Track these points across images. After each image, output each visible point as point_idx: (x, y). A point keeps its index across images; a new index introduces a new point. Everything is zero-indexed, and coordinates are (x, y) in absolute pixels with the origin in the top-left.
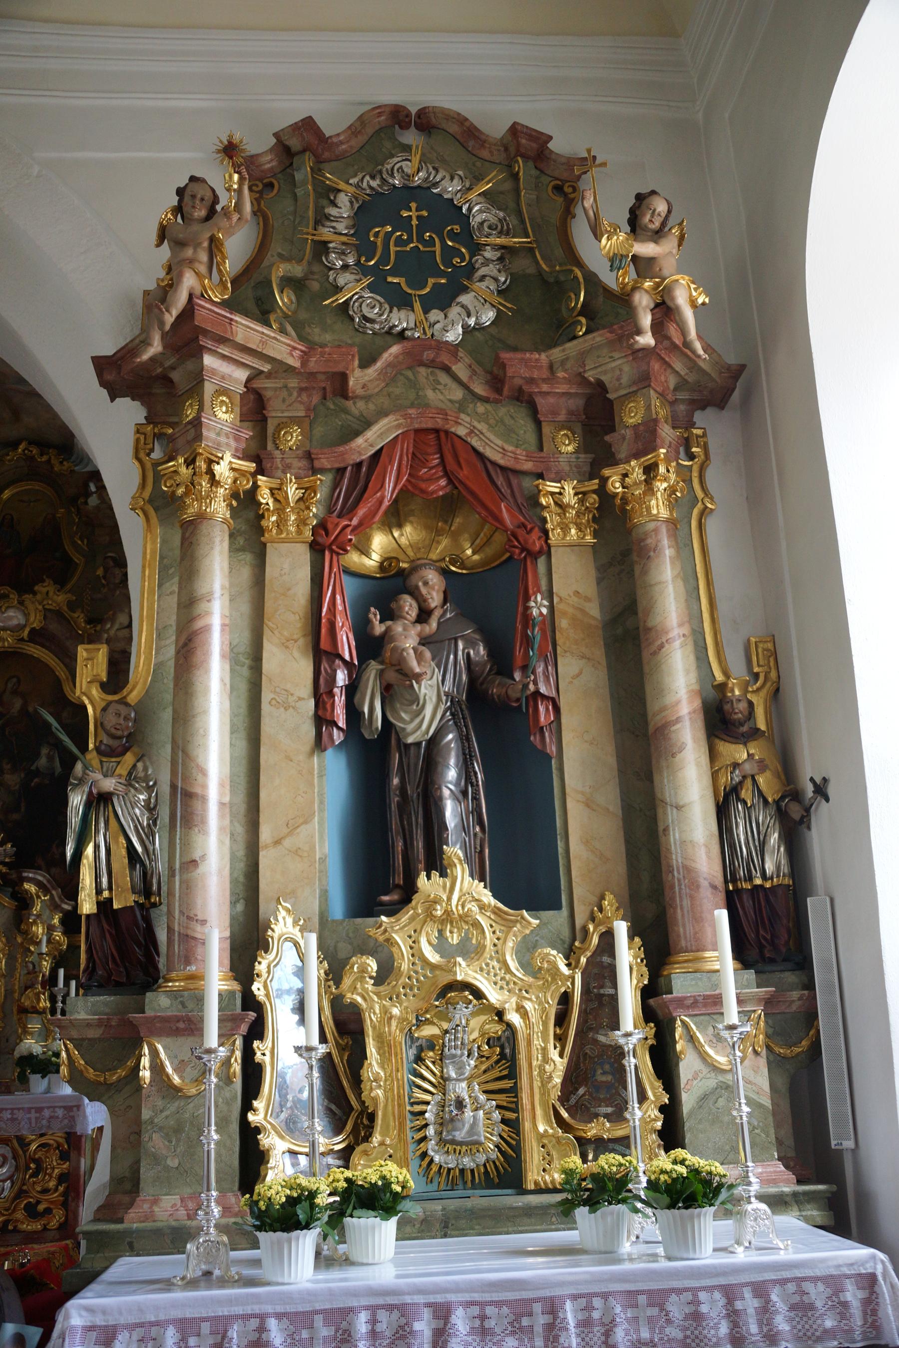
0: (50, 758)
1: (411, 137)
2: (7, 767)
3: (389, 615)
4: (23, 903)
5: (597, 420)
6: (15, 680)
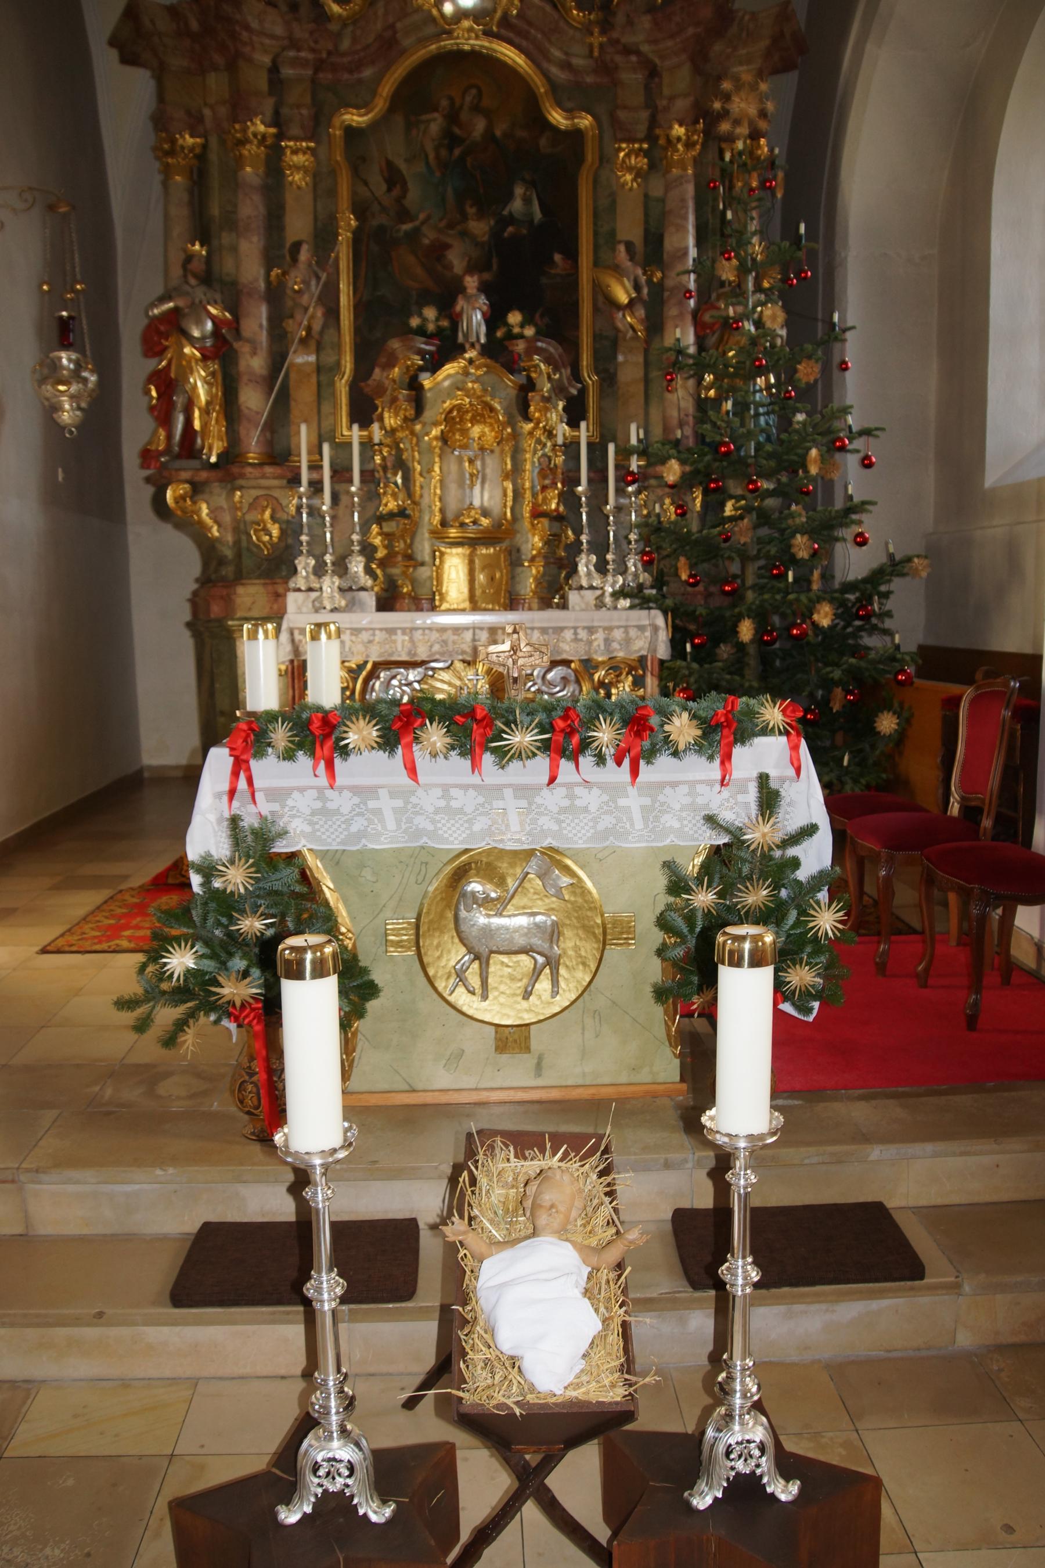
0: (527, 201)
2: (471, 211)
6: (474, 91)
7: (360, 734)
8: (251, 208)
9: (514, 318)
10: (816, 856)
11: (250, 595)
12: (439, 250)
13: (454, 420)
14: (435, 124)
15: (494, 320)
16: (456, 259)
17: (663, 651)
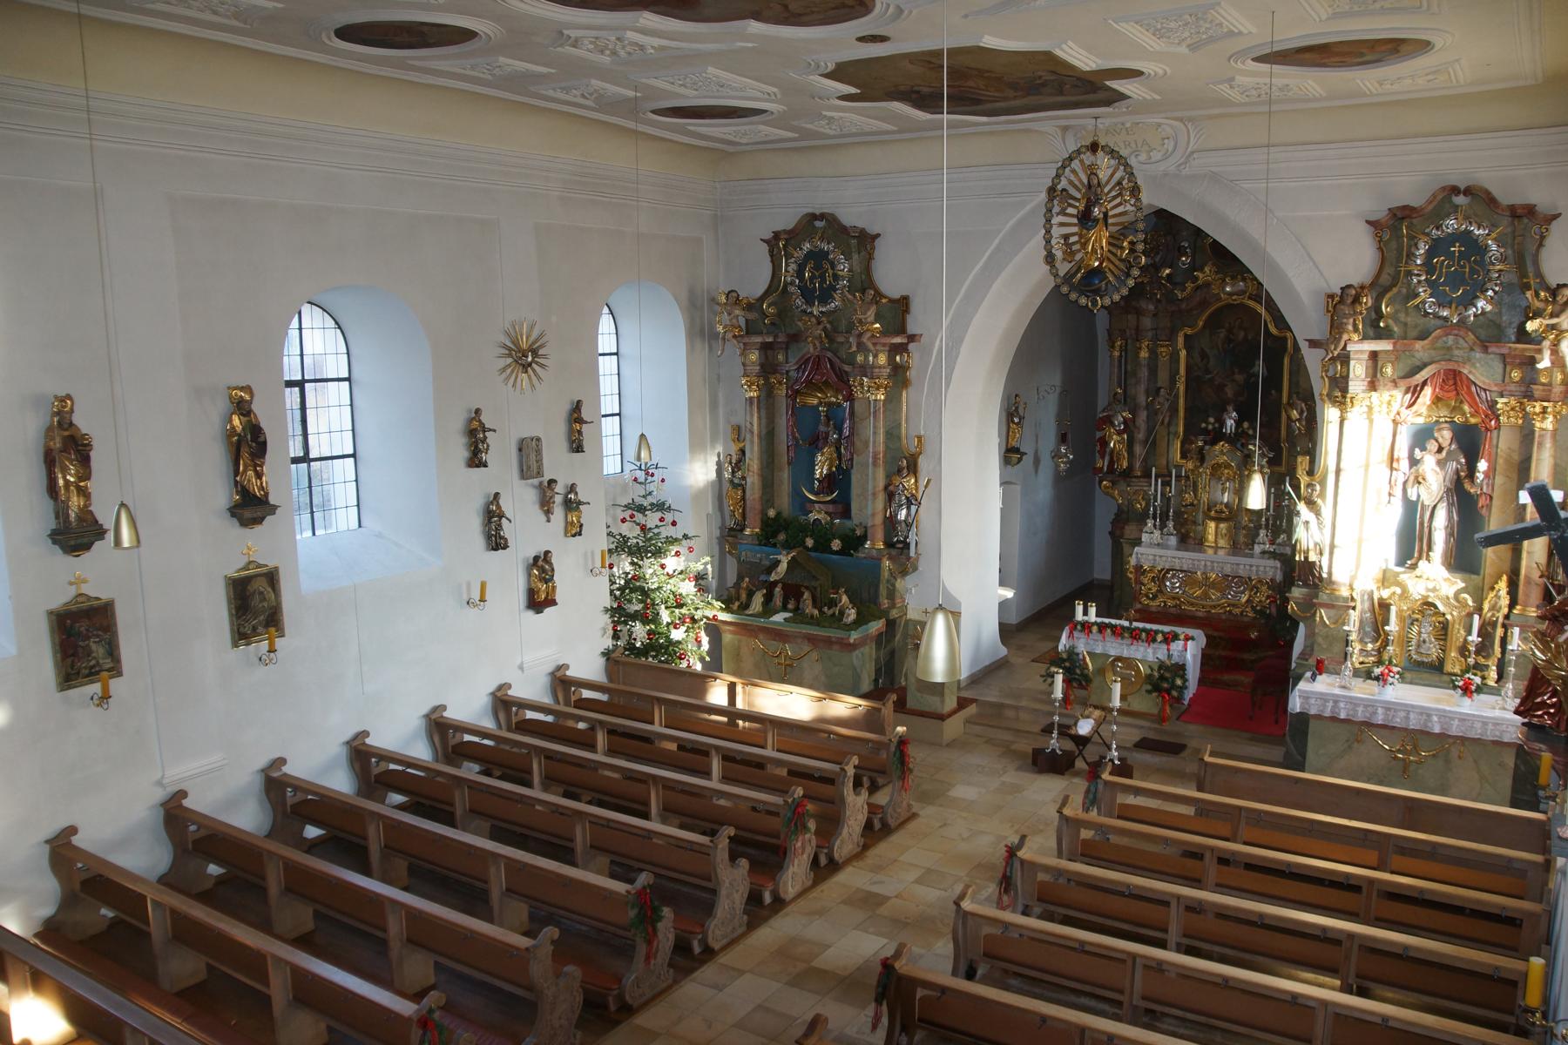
3: (1423, 449)
4: (1248, 457)
7: (1095, 629)
8: (1144, 373)
9: (1246, 425)
11: (1130, 531)
12: (1221, 387)
13: (1216, 468)
14: (1222, 333)
15: (1238, 423)
16: (1229, 391)
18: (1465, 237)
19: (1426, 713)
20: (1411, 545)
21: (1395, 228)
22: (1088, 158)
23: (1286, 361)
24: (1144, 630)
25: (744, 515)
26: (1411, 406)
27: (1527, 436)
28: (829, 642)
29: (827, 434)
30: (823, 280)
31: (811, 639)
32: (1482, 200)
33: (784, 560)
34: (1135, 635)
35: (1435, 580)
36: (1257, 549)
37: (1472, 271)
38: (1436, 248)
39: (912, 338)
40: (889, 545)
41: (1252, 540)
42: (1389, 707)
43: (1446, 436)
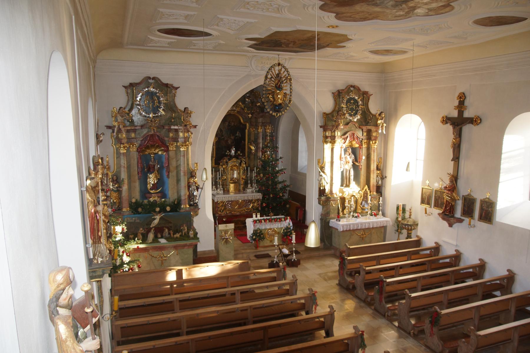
1: (352, 89)
5: (369, 132)
10: (292, 228)
12: (227, 140)
14: (227, 123)
15: (236, 152)
16: (229, 142)
17: (261, 198)
18: (354, 99)
19: (369, 223)
20: (345, 182)
21: (338, 95)
22: (277, 68)
23: (247, 131)
24: (277, 218)
25: (120, 203)
26: (344, 143)
27: (369, 148)
28: (184, 246)
29: (154, 166)
30: (154, 104)
31: (175, 247)
32: (357, 89)
33: (158, 217)
34: (276, 220)
35: (354, 190)
36: (249, 191)
37: (356, 108)
38: (349, 101)
39: (195, 127)
40: (190, 205)
41: (244, 189)
42: (362, 224)
43: (350, 151)
